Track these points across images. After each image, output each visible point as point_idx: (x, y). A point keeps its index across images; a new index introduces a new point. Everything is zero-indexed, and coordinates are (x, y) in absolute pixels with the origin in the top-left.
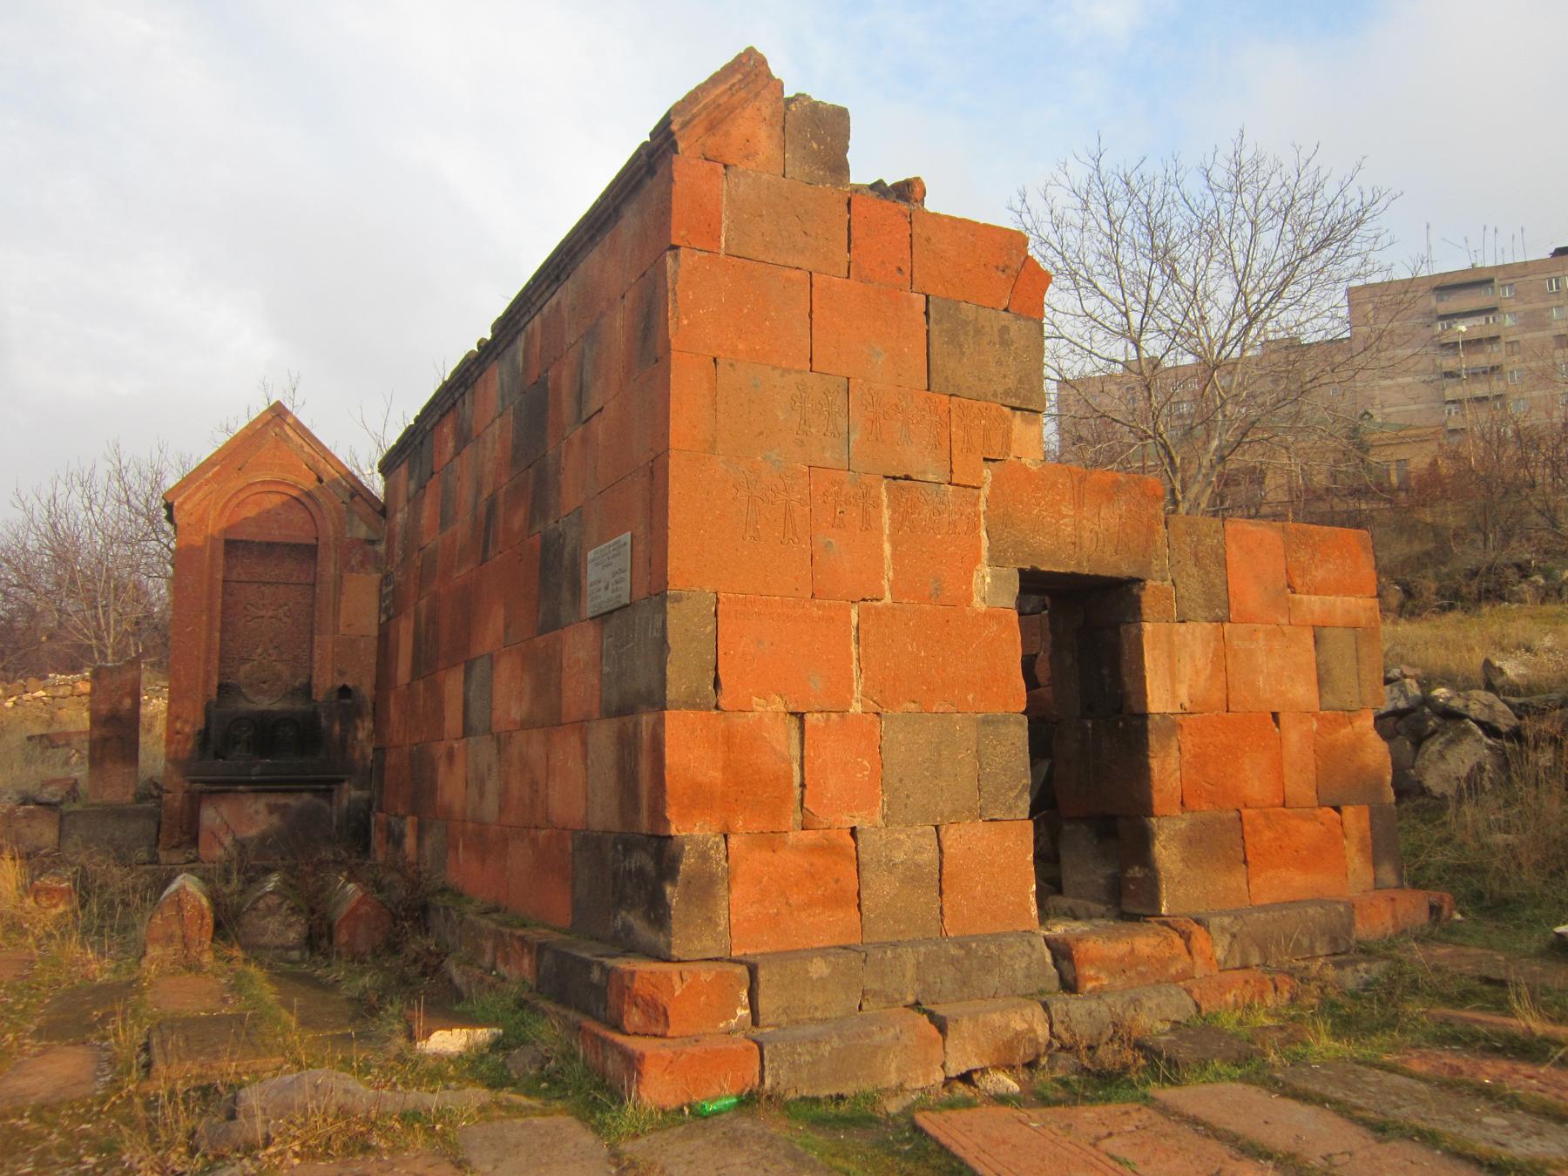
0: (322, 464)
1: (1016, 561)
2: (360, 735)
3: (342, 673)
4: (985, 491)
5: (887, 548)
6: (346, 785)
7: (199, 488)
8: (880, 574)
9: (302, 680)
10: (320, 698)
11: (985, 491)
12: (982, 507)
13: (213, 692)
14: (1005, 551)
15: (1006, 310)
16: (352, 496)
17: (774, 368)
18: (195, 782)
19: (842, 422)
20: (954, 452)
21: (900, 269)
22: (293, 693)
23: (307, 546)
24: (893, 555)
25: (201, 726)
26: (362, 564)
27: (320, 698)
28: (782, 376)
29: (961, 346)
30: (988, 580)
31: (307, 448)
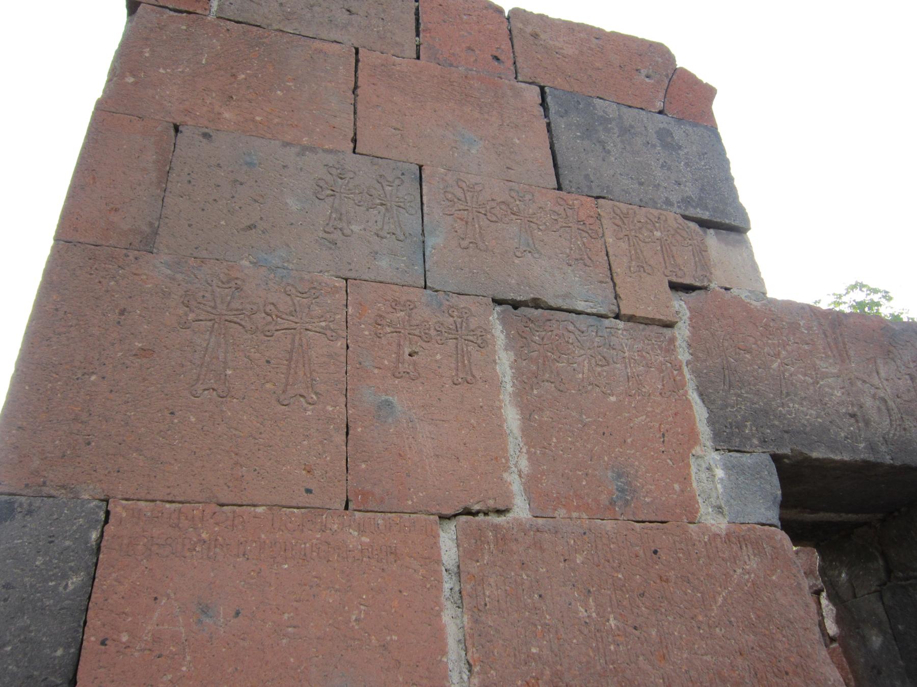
1: (763, 442)
4: (682, 332)
5: (512, 418)
8: (499, 461)
11: (682, 332)
12: (683, 356)
14: (740, 426)
15: (660, 112)
17: (286, 144)
19: (412, 222)
20: (616, 269)
21: (497, 58)
24: (526, 431)
28: (301, 154)
29: (602, 143)
30: (720, 473)
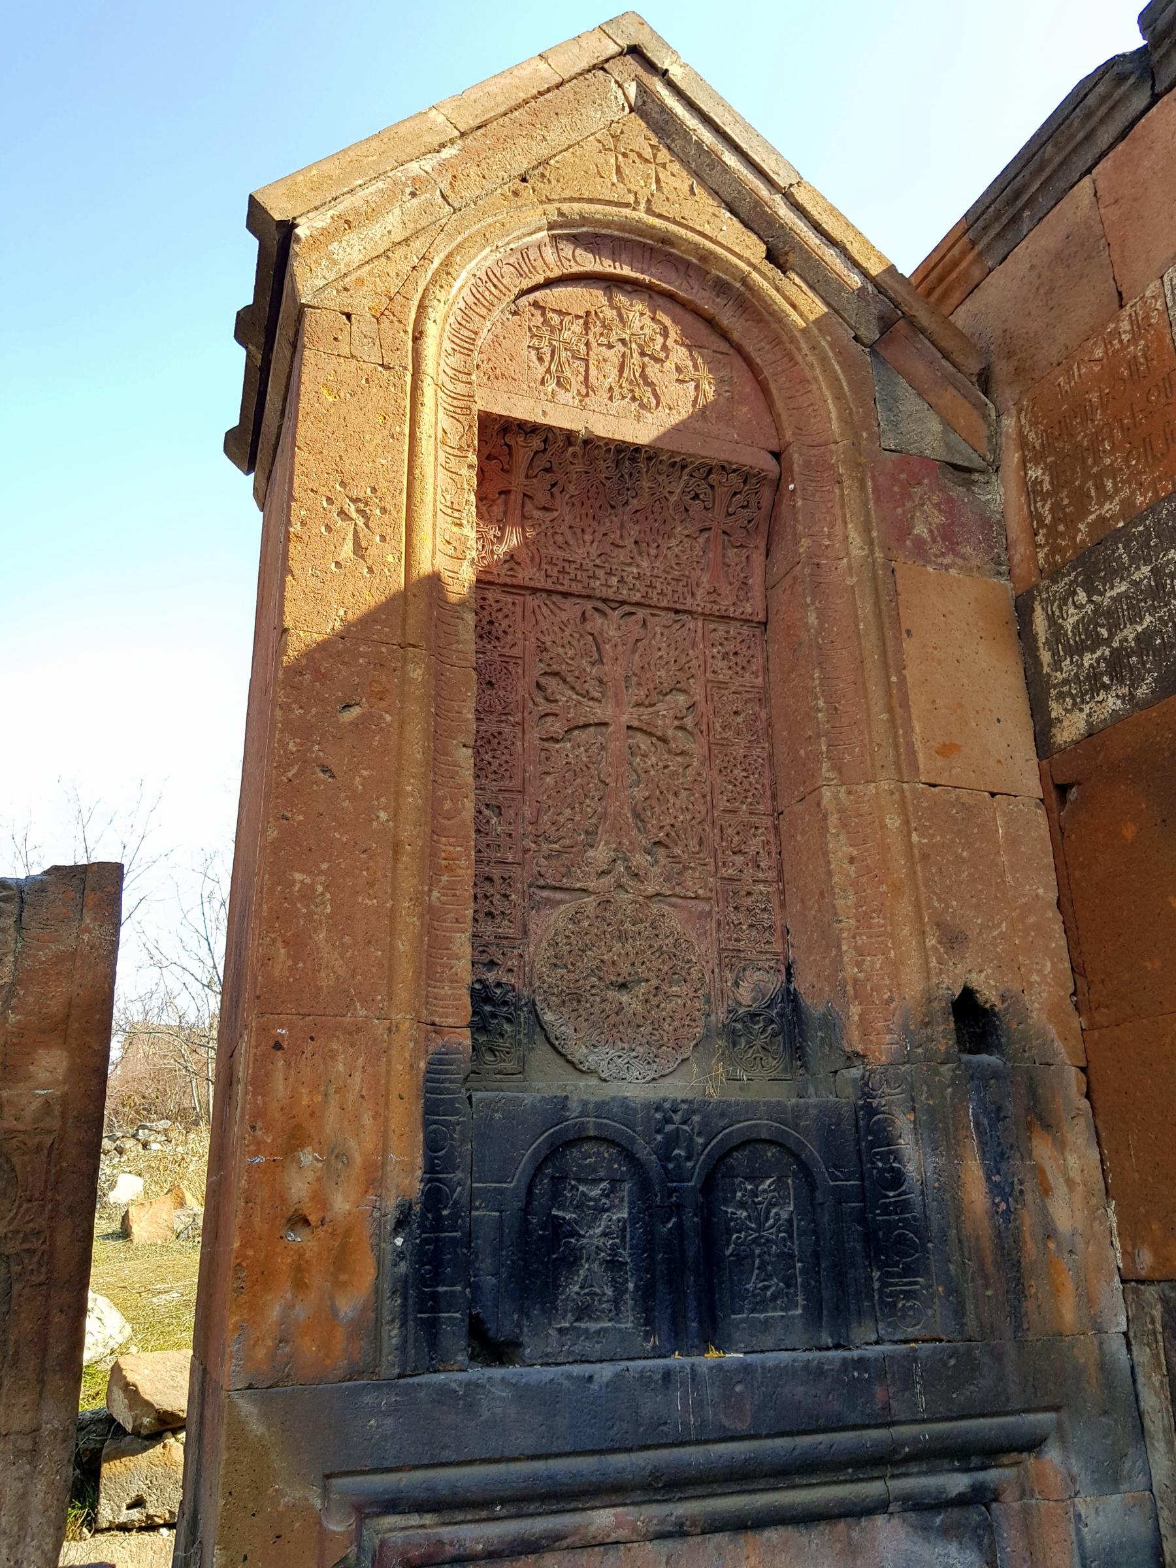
0: (784, 212)
2: (1066, 1212)
3: (954, 940)
6: (1053, 1454)
7: (389, 198)
9: (773, 983)
10: (883, 1047)
13: (456, 1009)
16: (886, 325)
18: (392, 1505)
22: (737, 1031)
23: (747, 476)
25: (406, 1180)
26: (948, 537)
27: (883, 1047)
31: (730, 159)
